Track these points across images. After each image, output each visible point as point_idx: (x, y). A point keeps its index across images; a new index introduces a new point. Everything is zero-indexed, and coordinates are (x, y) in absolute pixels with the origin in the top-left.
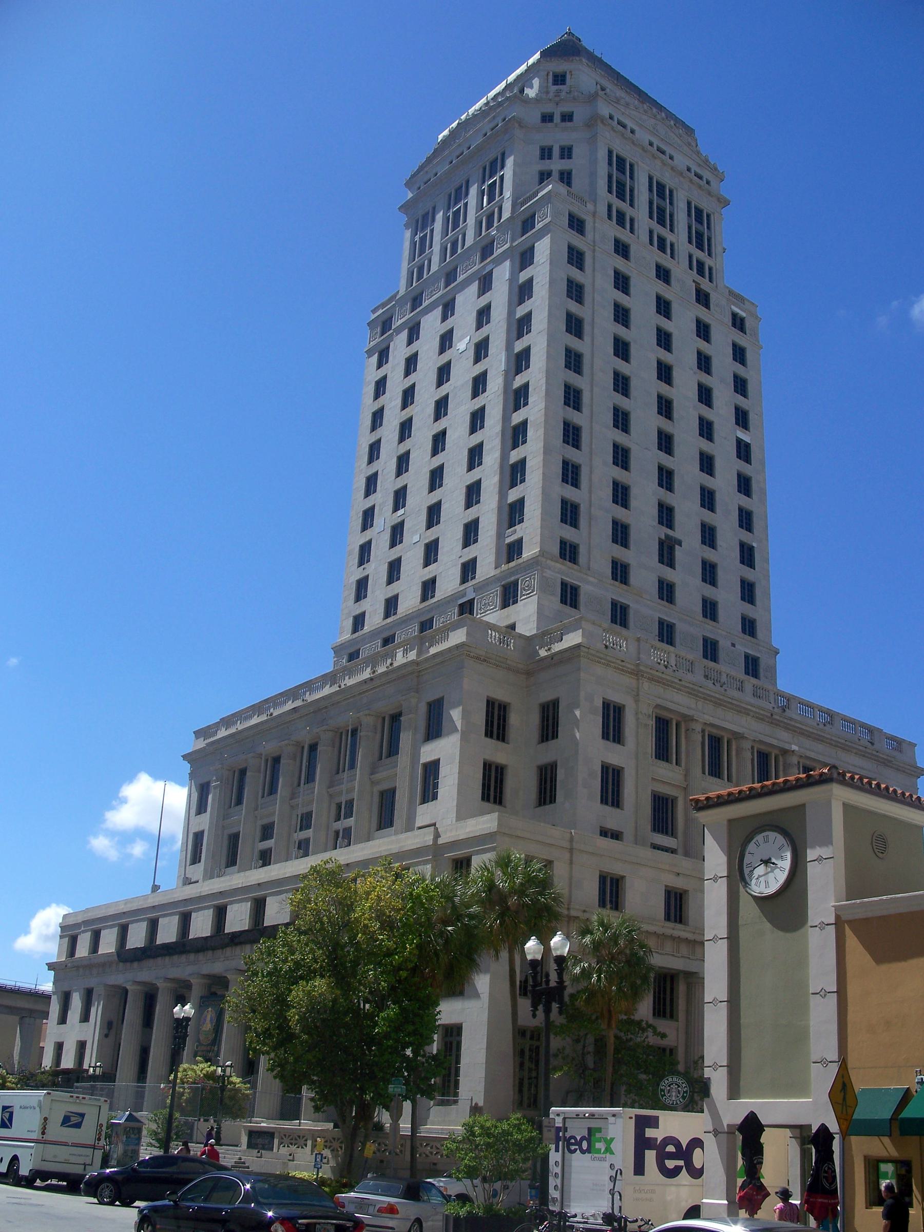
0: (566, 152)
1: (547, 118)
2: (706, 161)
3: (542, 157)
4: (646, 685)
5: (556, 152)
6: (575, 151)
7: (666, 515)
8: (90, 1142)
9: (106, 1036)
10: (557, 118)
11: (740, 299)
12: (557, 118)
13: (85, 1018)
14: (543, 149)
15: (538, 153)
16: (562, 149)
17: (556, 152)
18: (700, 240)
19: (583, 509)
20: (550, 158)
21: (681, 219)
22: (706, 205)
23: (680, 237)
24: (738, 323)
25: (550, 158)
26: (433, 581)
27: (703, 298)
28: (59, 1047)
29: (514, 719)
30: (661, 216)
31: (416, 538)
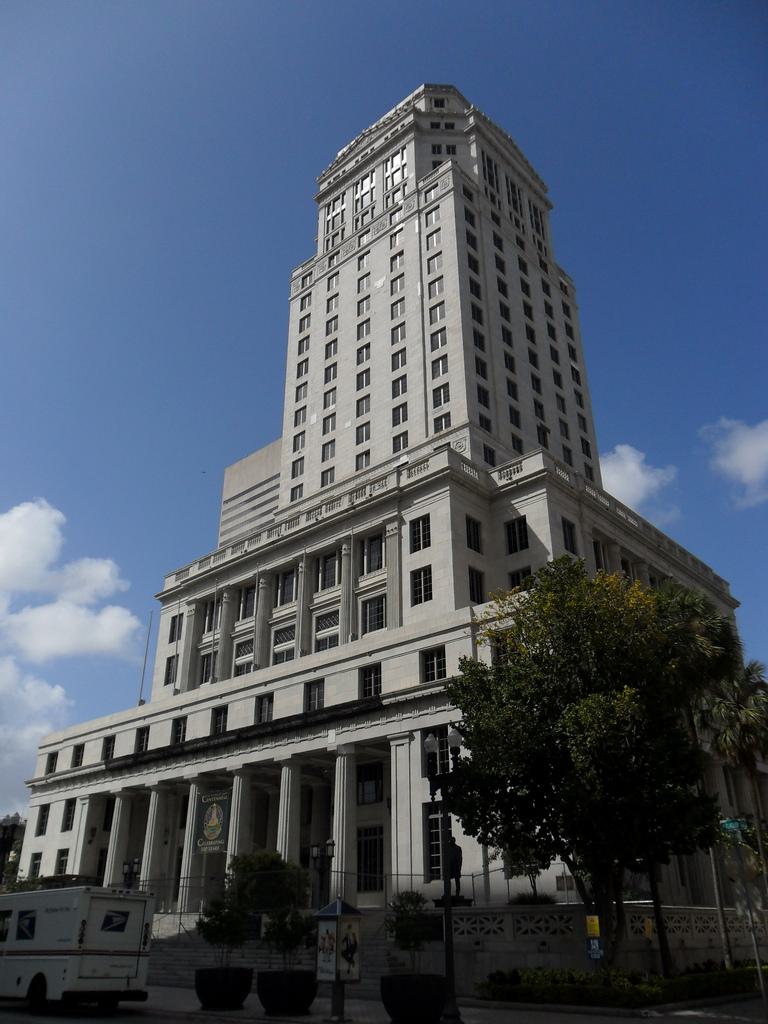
0: (451, 150)
1: (435, 126)
2: (537, 177)
3: (434, 152)
4: (586, 511)
5: (444, 149)
6: (458, 149)
7: (539, 408)
8: (135, 948)
9: (90, 842)
10: (443, 126)
11: (561, 272)
12: (443, 126)
13: (67, 826)
14: (434, 147)
15: (430, 149)
16: (448, 148)
17: (444, 149)
18: (538, 227)
19: (491, 395)
20: (439, 153)
21: (526, 209)
22: (541, 206)
23: (527, 221)
24: (563, 288)
25: (439, 153)
26: (367, 453)
27: (544, 266)
28: (37, 857)
29: (485, 535)
30: (515, 203)
31: (348, 424)
